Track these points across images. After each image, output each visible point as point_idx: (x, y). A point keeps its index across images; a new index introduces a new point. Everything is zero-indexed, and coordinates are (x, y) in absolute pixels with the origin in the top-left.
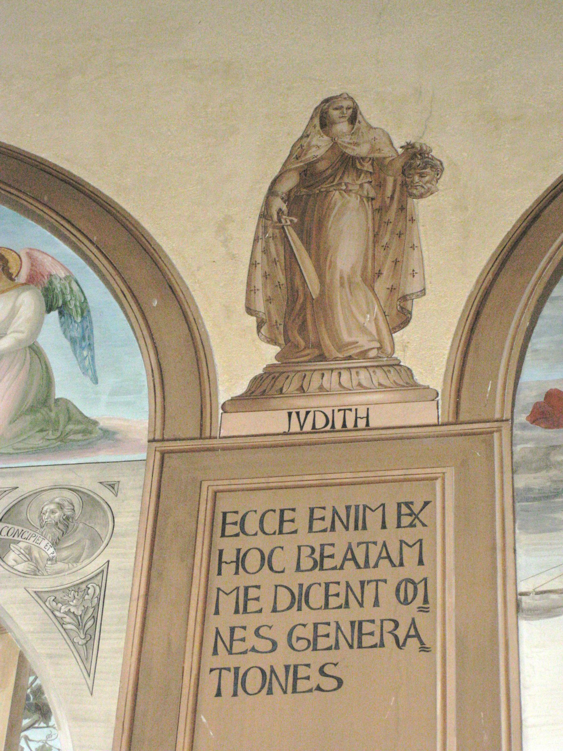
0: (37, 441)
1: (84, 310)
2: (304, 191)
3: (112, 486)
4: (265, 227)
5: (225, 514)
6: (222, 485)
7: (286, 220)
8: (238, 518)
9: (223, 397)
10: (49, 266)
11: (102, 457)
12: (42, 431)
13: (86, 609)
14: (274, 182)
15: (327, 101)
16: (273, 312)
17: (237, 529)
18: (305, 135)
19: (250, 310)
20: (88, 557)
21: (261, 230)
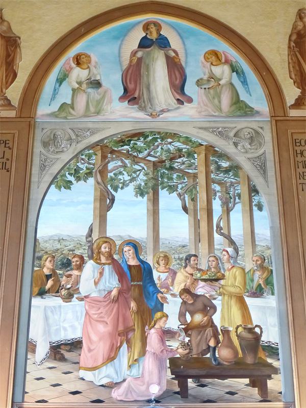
0: (238, 113)
1: (243, 73)
2: (299, 40)
3: (261, 128)
4: (290, 51)
5: (295, 139)
6: (293, 131)
7: (296, 49)
8: (299, 141)
9: (289, 105)
10: (230, 58)
11: (257, 119)
12: (239, 110)
13: (262, 164)
14: (290, 36)
15: (300, 10)
16: (297, 78)
17: (299, 144)
18: (296, 22)
19: (291, 78)
20: (260, 148)
21: (289, 52)
